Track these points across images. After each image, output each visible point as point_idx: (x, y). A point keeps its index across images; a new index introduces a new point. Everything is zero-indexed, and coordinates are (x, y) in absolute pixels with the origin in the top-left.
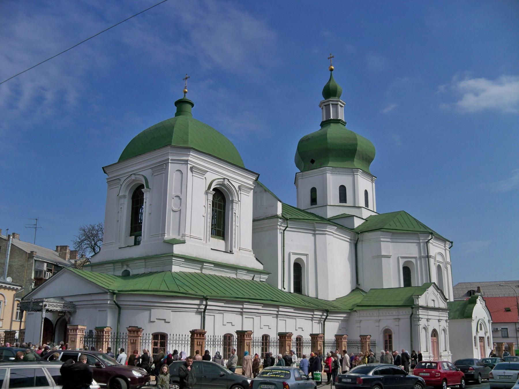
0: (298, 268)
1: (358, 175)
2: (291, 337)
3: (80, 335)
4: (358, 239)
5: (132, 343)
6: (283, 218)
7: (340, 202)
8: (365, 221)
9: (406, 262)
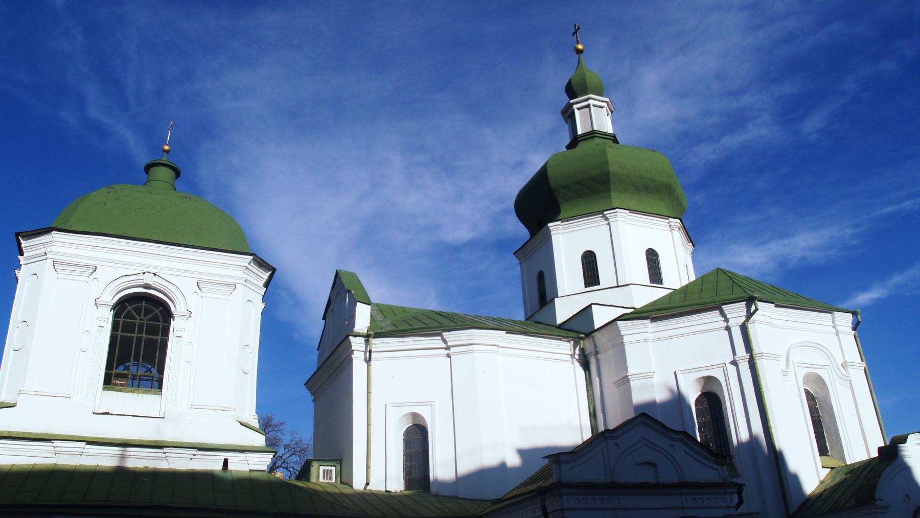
1: (618, 222)
7: (586, 286)
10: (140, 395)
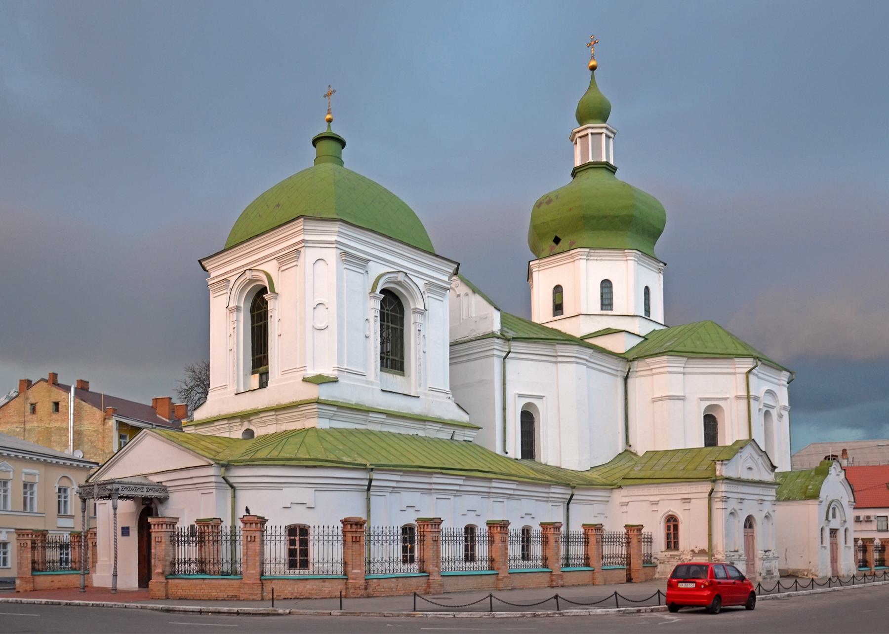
0: (528, 419)
2: (507, 527)
3: (170, 533)
4: (629, 369)
6: (503, 337)
7: (602, 309)
8: (643, 339)
9: (710, 407)
10: (394, 375)
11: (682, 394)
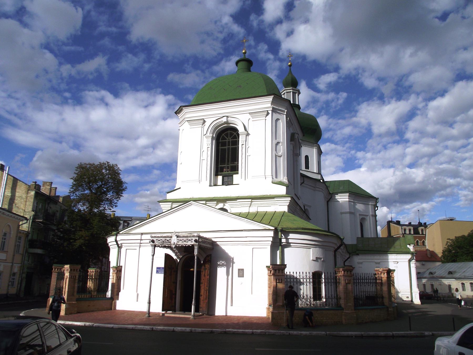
4: (331, 197)
5: (347, 283)
11: (353, 211)
